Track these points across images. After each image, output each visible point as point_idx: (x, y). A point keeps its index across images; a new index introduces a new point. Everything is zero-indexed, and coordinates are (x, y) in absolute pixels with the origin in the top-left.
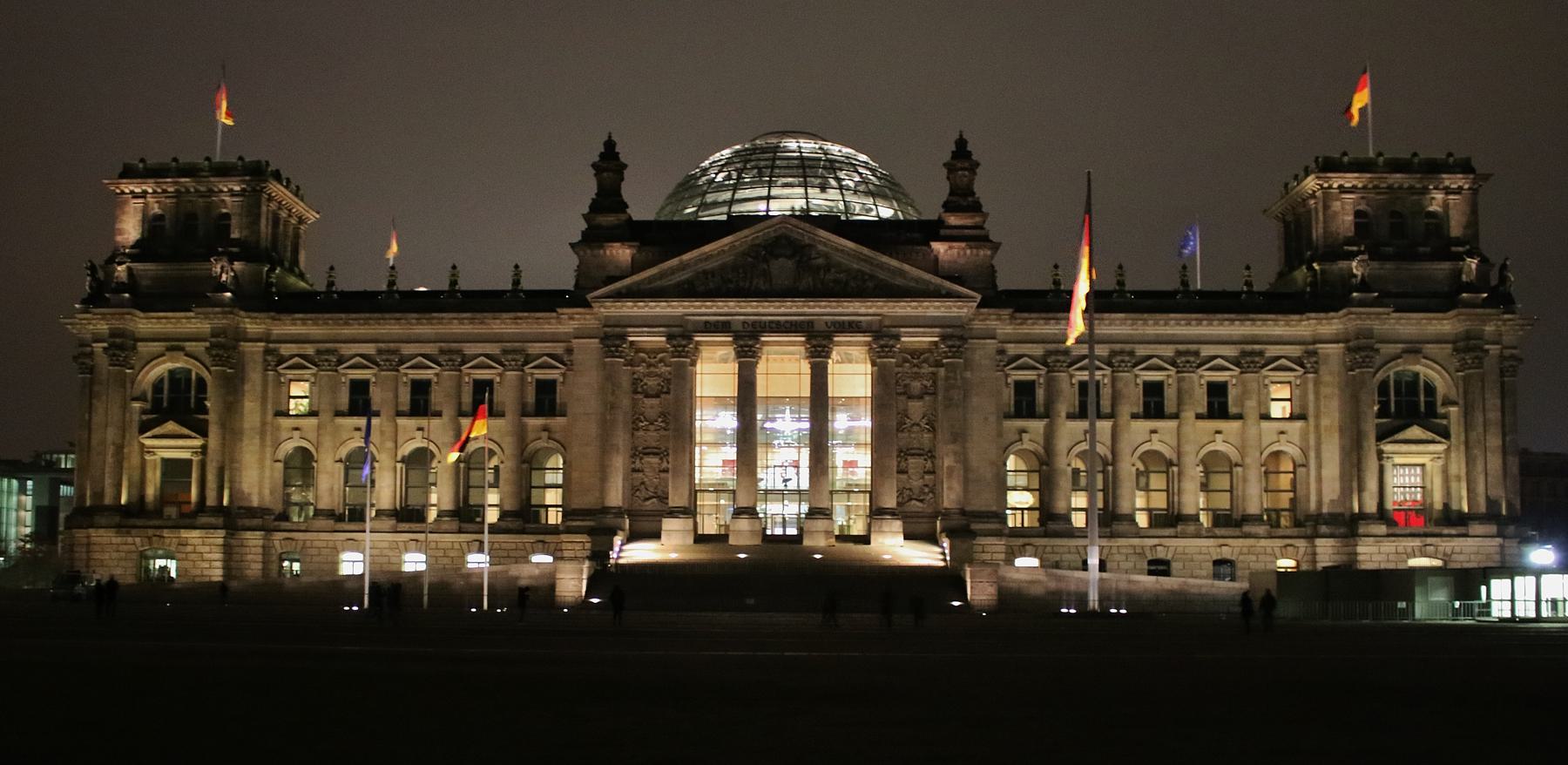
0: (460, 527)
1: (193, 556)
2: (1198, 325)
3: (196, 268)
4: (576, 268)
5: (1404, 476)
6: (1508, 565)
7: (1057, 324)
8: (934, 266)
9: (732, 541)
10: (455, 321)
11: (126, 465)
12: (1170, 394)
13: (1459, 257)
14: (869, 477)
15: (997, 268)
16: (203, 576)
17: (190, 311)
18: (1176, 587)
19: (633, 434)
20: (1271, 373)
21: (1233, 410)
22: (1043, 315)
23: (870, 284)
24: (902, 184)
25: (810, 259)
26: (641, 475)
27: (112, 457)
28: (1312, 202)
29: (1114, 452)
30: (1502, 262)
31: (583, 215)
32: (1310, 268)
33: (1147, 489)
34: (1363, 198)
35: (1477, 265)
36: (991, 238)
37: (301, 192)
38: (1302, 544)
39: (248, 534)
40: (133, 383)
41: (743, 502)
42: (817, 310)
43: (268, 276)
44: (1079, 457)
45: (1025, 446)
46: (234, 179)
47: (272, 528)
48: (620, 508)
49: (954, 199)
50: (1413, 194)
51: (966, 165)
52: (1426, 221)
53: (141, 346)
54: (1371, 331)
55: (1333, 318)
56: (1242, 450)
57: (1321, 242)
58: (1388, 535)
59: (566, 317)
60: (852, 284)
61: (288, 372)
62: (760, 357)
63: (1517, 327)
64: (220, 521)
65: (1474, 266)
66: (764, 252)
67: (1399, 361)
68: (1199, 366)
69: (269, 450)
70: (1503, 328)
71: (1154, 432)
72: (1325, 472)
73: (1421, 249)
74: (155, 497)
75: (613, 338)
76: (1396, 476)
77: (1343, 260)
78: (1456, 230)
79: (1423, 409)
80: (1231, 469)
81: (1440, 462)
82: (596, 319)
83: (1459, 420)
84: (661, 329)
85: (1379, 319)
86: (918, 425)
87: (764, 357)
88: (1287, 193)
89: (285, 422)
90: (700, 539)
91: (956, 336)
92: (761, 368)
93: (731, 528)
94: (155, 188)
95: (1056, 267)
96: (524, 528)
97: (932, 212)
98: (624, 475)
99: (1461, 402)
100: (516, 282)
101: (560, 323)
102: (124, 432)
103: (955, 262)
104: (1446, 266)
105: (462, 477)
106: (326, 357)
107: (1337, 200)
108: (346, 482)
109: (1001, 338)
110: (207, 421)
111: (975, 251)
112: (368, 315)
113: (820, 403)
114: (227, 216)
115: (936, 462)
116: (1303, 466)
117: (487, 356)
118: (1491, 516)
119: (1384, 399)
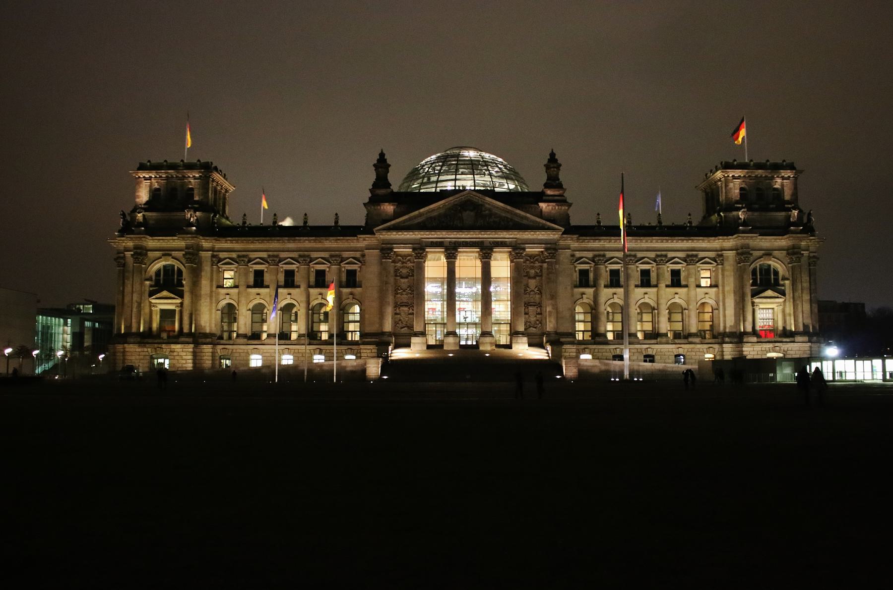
0: (310, 343)
1: (177, 358)
2: (666, 242)
3: (179, 214)
4: (366, 215)
5: (763, 314)
6: (813, 356)
7: (599, 242)
8: (540, 214)
9: (445, 348)
10: (307, 241)
11: (142, 312)
12: (653, 275)
13: (789, 210)
14: (510, 316)
15: (570, 215)
16: (182, 367)
17: (176, 236)
18: (661, 368)
19: (395, 296)
20: (701, 265)
21: (683, 283)
22: (593, 238)
24: (519, 173)
26: (399, 316)
27: (136, 308)
28: (720, 183)
30: (808, 212)
31: (370, 189)
32: (719, 215)
33: (641, 321)
35: (798, 214)
36: (568, 200)
37: (226, 177)
38: (716, 346)
39: (205, 346)
40: (146, 272)
41: (450, 330)
42: (486, 236)
43: (213, 219)
44: (610, 307)
45: (584, 301)
47: (216, 343)
48: (390, 332)
49: (549, 182)
50: (766, 180)
51: (555, 165)
52: (773, 192)
53: (150, 254)
54: (748, 244)
55: (730, 239)
56: (688, 302)
57: (724, 202)
58: (758, 342)
59: (362, 239)
60: (502, 223)
61: (223, 266)
62: (457, 259)
63: (816, 243)
64: (191, 340)
65: (796, 214)
66: (459, 208)
67: (762, 259)
68: (667, 262)
69: (214, 305)
70: (810, 244)
71: (646, 293)
72: (726, 312)
73: (771, 206)
74: (157, 328)
75: (386, 250)
76: (760, 314)
77: (734, 211)
78: (787, 196)
79: (772, 282)
80: (682, 311)
81: (781, 307)
82: (376, 240)
83: (790, 286)
84: (410, 245)
85: (752, 239)
86: (533, 291)
87: (458, 258)
88: (707, 178)
90: (429, 347)
91: (552, 248)
92: (457, 263)
93: (445, 342)
94: (156, 175)
95: (598, 214)
96: (342, 342)
97: (538, 187)
98: (392, 316)
99: (791, 279)
100: (336, 222)
101: (358, 242)
102: (141, 296)
103: (550, 212)
104: (783, 214)
105: (310, 317)
106: (242, 259)
107: (732, 182)
108: (252, 320)
109: (572, 248)
110: (183, 290)
111: (560, 207)
112: (263, 238)
113: (486, 279)
114: (192, 189)
115: (542, 309)
116: (717, 309)
117: (322, 258)
118: (805, 332)
119: (754, 277)
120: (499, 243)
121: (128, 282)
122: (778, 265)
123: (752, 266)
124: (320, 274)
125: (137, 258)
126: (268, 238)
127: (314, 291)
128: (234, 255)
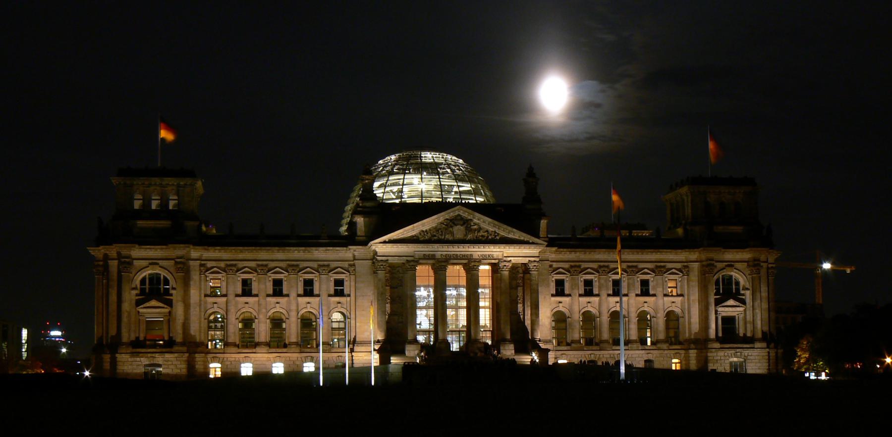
1: (172, 367)
7: (575, 254)
10: (296, 251)
21: (651, 292)
22: (569, 250)
23: (498, 238)
25: (471, 226)
38: (683, 352)
39: (197, 355)
40: (132, 281)
61: (210, 275)
64: (185, 349)
67: (725, 270)
69: (203, 314)
79: (734, 291)
89: (211, 300)
99: (751, 289)
110: (172, 300)
116: (683, 317)
120: (487, 256)
122: (741, 278)
123: (716, 277)
126: (258, 248)
127: (303, 300)
128: (222, 264)
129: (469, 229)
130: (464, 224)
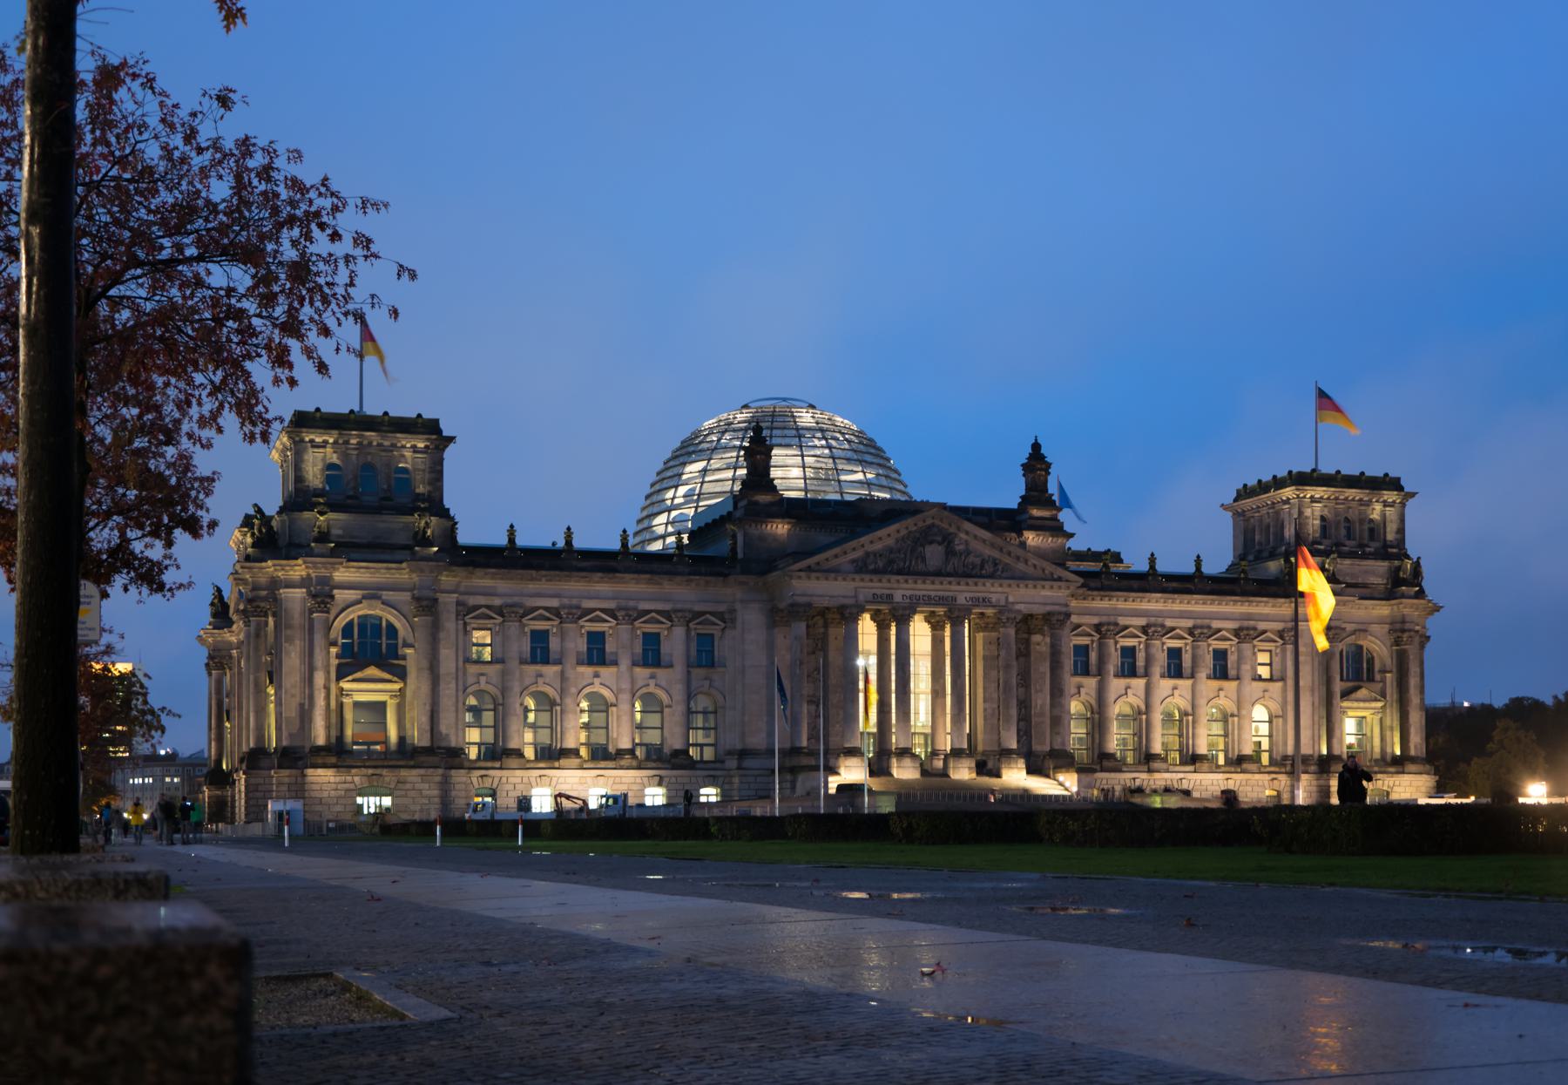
1: (412, 793)
20: (1259, 643)
21: (1232, 672)
22: (1102, 593)
28: (1287, 506)
29: (1148, 705)
34: (1325, 506)
46: (421, 436)
50: (1361, 505)
51: (1043, 466)
61: (473, 621)
81: (1380, 715)
99: (1394, 670)
110: (404, 667)
111: (1055, 539)
121: (292, 648)
124: (652, 641)
125: (323, 602)
129: (950, 552)
130: (944, 541)
